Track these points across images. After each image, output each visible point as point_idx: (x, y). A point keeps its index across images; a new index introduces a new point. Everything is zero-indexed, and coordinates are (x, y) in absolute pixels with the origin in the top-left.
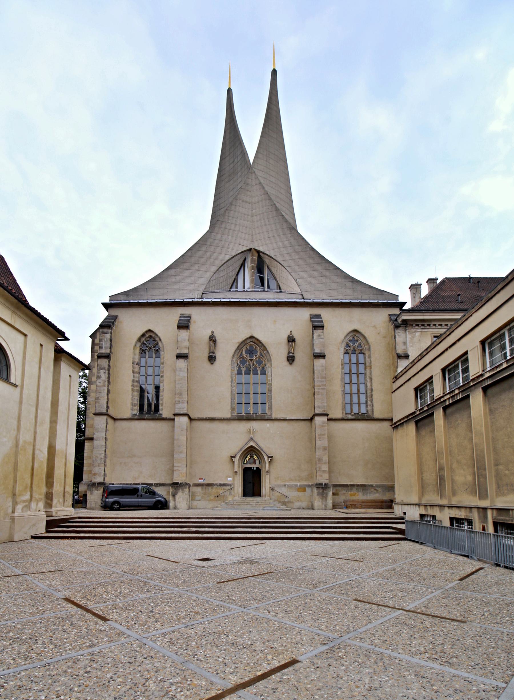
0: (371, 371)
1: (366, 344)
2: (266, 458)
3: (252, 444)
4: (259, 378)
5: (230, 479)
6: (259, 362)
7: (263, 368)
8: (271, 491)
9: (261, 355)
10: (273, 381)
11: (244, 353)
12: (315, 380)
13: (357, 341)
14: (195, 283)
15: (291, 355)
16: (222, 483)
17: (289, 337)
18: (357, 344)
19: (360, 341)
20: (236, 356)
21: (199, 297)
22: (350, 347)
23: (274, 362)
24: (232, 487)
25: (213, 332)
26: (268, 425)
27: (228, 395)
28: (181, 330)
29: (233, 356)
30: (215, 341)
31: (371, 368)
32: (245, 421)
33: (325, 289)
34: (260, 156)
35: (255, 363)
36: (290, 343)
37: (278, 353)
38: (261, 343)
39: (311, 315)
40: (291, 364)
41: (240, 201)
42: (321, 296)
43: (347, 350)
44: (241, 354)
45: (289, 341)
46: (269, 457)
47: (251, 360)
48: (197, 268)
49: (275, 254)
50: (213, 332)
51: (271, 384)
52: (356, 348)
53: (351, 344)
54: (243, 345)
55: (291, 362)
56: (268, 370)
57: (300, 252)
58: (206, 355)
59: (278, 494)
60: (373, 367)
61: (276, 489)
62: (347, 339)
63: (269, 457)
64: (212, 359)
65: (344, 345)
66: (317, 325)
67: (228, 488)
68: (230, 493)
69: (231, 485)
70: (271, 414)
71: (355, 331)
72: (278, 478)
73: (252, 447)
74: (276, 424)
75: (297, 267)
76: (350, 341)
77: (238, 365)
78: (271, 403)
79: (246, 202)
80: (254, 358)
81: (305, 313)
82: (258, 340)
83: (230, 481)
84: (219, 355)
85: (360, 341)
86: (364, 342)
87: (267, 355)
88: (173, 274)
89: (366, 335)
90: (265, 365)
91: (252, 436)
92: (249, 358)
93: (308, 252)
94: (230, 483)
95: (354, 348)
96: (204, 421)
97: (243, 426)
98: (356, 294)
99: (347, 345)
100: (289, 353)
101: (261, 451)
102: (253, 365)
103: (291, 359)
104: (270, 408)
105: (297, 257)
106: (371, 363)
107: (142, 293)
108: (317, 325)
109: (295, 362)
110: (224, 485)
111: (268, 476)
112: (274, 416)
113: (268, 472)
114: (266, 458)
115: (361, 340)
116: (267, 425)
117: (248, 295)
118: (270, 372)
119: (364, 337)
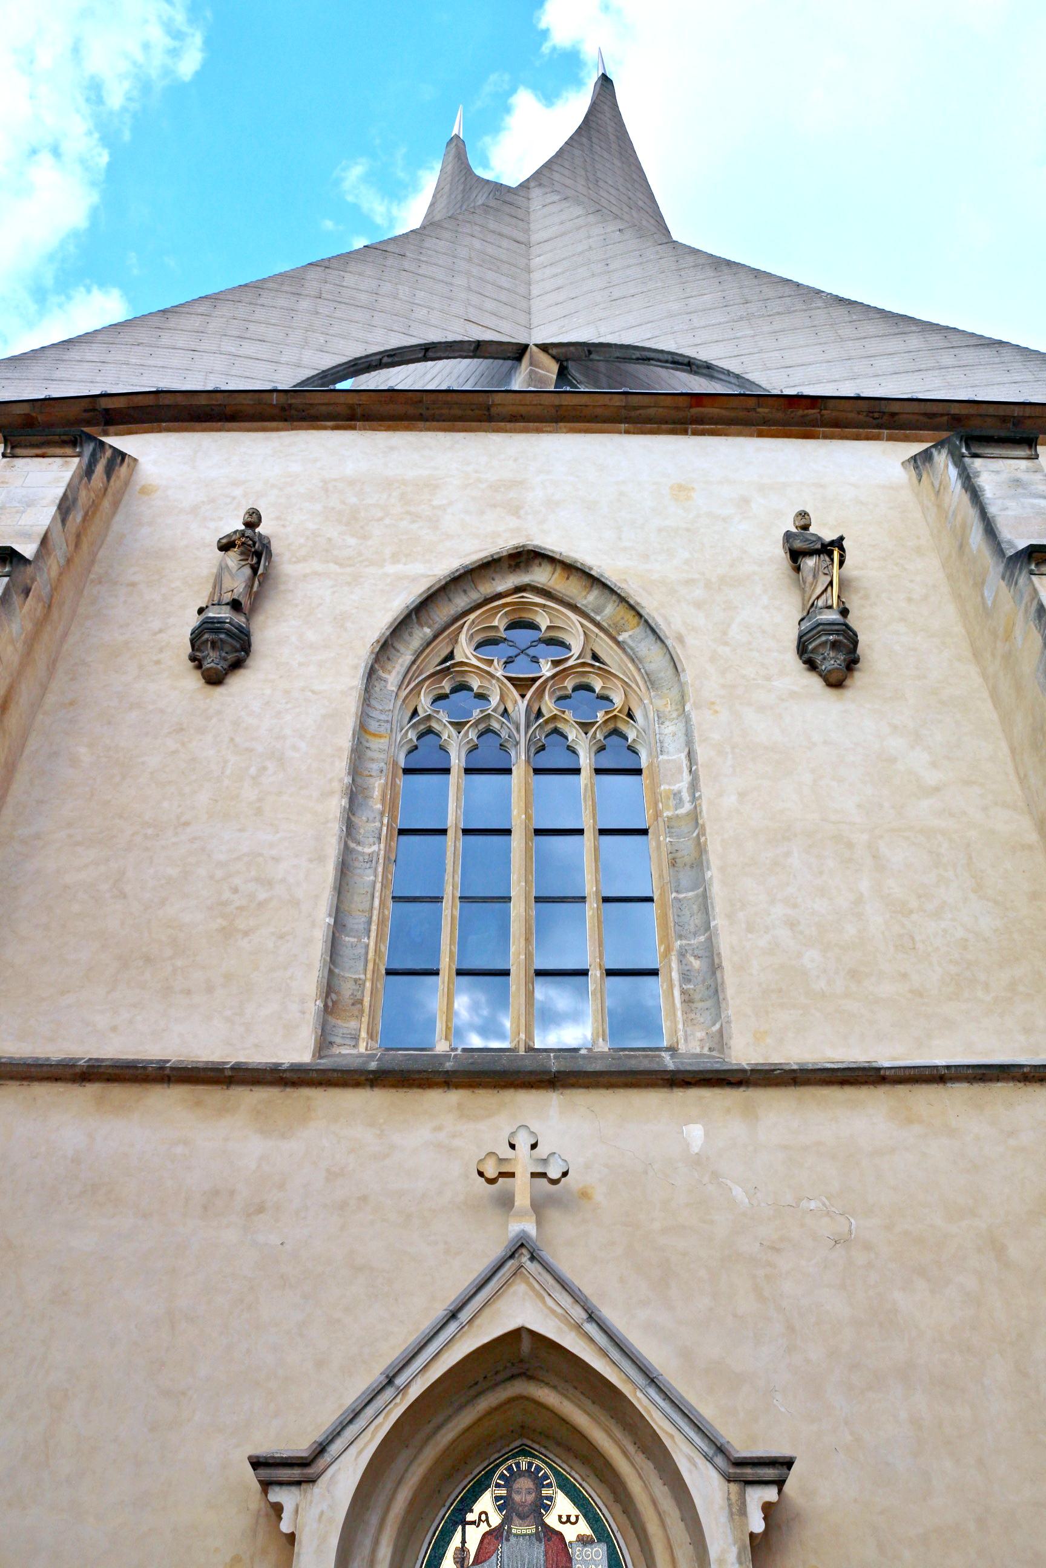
2: (706, 1484)
3: (521, 1310)
4: (583, 799)
6: (581, 686)
26: (695, 1133)
29: (385, 648)
32: (454, 1097)
35: (549, 706)
40: (836, 682)
45: (796, 556)
54: (461, 602)
56: (659, 739)
57: (778, 313)
73: (521, 1356)
74: (777, 1109)
82: (570, 568)
84: (275, 633)
87: (648, 649)
91: (526, 1225)
96: (40, 1090)
97: (438, 1142)
101: (642, 1400)
104: (708, 988)
109: (859, 678)
112: (743, 1054)
114: (706, 1484)
116: (693, 1126)
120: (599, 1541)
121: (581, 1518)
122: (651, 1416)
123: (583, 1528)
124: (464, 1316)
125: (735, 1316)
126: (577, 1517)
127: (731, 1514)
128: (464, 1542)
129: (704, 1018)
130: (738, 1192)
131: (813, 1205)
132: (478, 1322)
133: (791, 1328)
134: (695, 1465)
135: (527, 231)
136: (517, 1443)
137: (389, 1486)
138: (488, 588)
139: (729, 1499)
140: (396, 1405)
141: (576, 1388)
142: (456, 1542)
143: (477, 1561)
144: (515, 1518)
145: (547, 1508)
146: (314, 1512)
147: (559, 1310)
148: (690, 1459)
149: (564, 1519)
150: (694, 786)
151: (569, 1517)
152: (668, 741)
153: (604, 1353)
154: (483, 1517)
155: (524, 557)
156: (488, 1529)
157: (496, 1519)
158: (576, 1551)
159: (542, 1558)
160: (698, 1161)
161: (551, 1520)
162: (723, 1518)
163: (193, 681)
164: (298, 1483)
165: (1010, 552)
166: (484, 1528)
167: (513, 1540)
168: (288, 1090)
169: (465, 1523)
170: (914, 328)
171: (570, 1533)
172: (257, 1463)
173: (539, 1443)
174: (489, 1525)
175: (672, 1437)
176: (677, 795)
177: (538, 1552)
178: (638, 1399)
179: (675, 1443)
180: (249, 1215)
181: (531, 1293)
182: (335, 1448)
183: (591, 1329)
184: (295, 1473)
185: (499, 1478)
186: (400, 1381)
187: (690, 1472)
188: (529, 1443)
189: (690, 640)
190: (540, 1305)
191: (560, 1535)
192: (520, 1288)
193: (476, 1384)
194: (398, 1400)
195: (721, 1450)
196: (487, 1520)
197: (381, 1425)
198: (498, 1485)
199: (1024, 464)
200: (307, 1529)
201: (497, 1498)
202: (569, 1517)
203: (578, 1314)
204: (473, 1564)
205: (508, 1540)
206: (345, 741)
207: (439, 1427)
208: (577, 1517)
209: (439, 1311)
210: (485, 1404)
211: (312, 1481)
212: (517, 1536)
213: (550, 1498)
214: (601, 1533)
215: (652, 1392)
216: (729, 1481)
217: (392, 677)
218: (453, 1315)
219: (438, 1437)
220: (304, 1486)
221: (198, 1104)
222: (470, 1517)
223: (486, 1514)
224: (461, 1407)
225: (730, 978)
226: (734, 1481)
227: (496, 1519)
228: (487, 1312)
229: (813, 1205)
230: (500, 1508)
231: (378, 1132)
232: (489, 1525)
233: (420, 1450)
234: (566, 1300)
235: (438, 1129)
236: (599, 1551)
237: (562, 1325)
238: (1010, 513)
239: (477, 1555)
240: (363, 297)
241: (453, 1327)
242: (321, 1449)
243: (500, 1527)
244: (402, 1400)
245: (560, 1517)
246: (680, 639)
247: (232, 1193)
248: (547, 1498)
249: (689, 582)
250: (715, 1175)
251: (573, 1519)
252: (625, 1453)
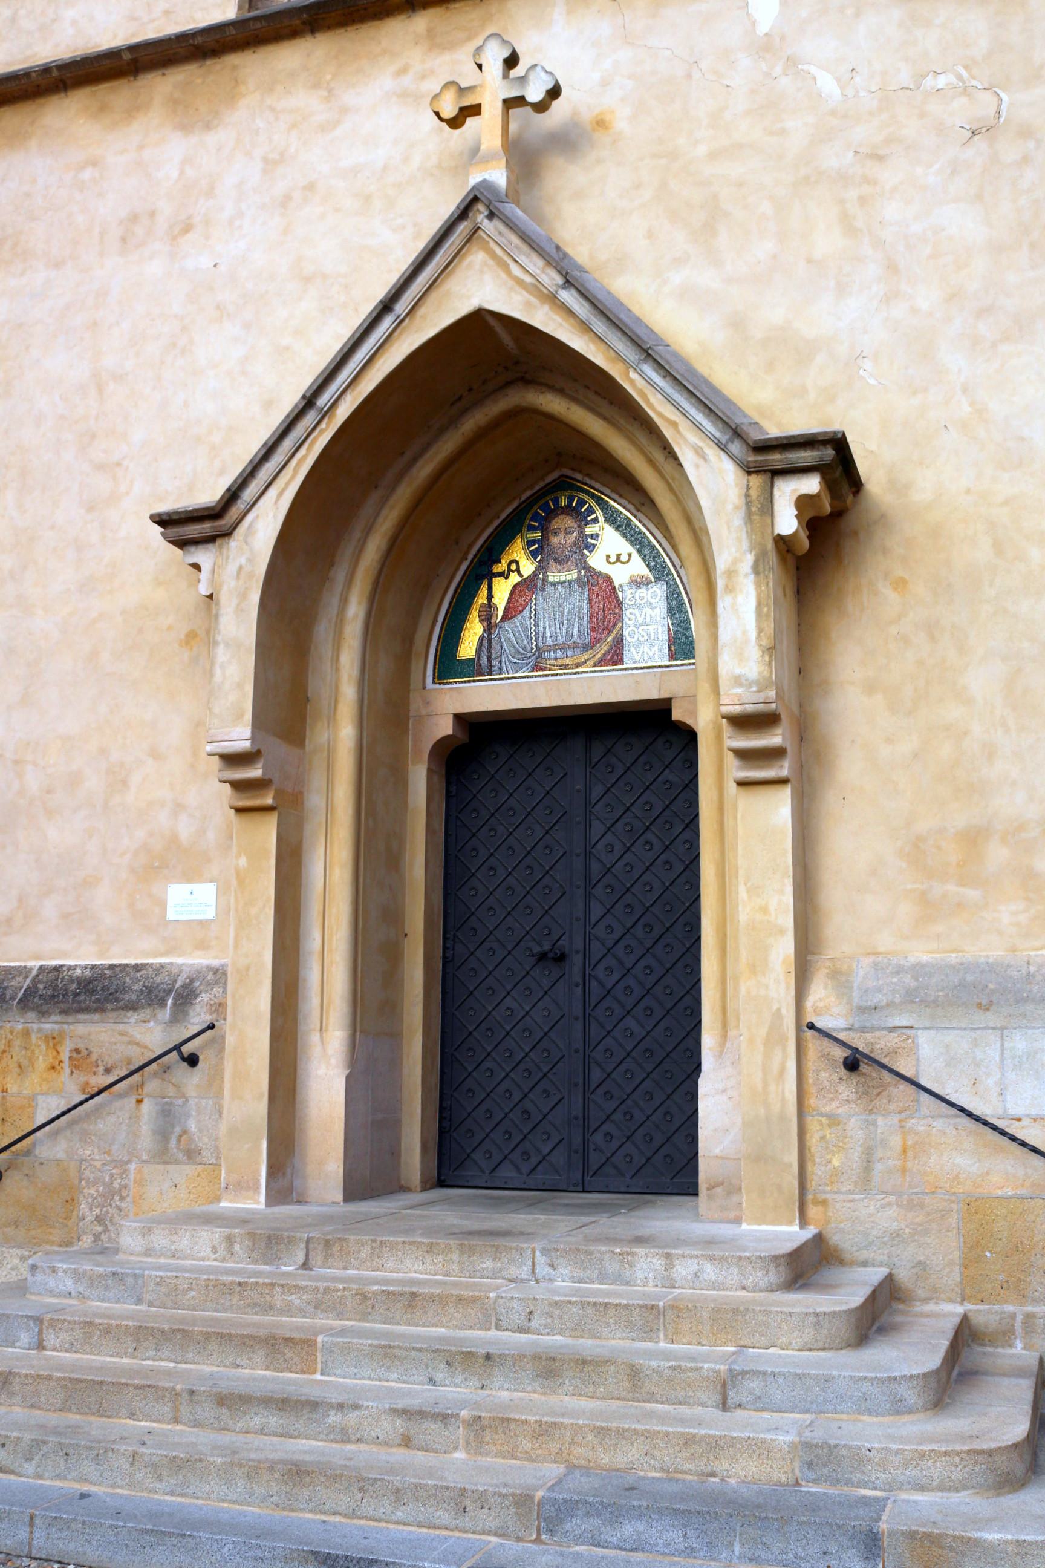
2: (715, 480)
5: (191, 900)
8: (838, 1095)
16: (80, 955)
24: (198, 1018)
46: (768, 458)
59: (962, 1162)
61: (931, 1055)
63: (768, 458)
67: (150, 1033)
68: (168, 1119)
69: (186, 996)
72: (973, 839)
83: (199, 931)
94: (189, 960)
101: (640, 384)
110: (95, 992)
111: (779, 808)
113: (788, 738)
120: (658, 579)
121: (636, 556)
122: (647, 401)
123: (638, 567)
124: (401, 307)
125: (809, 261)
126: (630, 555)
127: (749, 514)
128: (490, 596)
130: (827, 84)
131: (942, 82)
132: (422, 311)
133: (892, 268)
134: (704, 457)
136: (555, 475)
137: (357, 535)
139: (747, 496)
140: (322, 431)
141: (587, 387)
142: (482, 599)
143: (506, 617)
144: (552, 562)
145: (591, 548)
146: (232, 568)
147: (528, 279)
148: (699, 452)
149: (613, 559)
151: (618, 556)
153: (585, 327)
154: (514, 567)
156: (519, 579)
157: (528, 567)
158: (627, 595)
159: (585, 607)
160: (766, 47)
161: (596, 561)
162: (738, 520)
164: (211, 539)
166: (514, 578)
167: (549, 589)
168: (209, 62)
169: (491, 576)
171: (620, 575)
172: (164, 521)
173: (580, 472)
174: (520, 575)
175: (674, 424)
177: (580, 600)
178: (632, 382)
179: (678, 432)
180: (174, 238)
181: (491, 262)
182: (248, 494)
183: (567, 296)
184: (205, 528)
185: (532, 520)
186: (323, 401)
187: (697, 466)
188: (569, 473)
190: (503, 275)
191: (608, 579)
192: (477, 257)
193: (460, 398)
194: (323, 425)
195: (737, 433)
196: (518, 570)
197: (304, 458)
198: (532, 529)
200: (225, 588)
201: (530, 543)
202: (618, 556)
203: (551, 279)
204: (502, 620)
205: (543, 589)
207: (415, 459)
208: (630, 555)
209: (367, 308)
210: (470, 424)
211: (228, 534)
212: (554, 584)
213: (596, 536)
214: (660, 572)
215: (648, 369)
216: (749, 473)
218: (386, 307)
219: (414, 471)
220: (219, 541)
221: (103, 108)
222: (497, 569)
223: (517, 563)
224: (442, 430)
226: (757, 472)
227: (528, 567)
228: (433, 296)
229: (942, 82)
230: (534, 554)
231: (325, 93)
232: (520, 575)
233: (393, 488)
234: (535, 264)
235: (403, 71)
236: (658, 593)
237: (532, 299)
239: (506, 610)
241: (387, 323)
242: (232, 495)
243: (535, 575)
244: (328, 425)
245: (608, 556)
247: (152, 214)
248: (592, 536)
250: (792, 62)
251: (624, 558)
252: (651, 462)
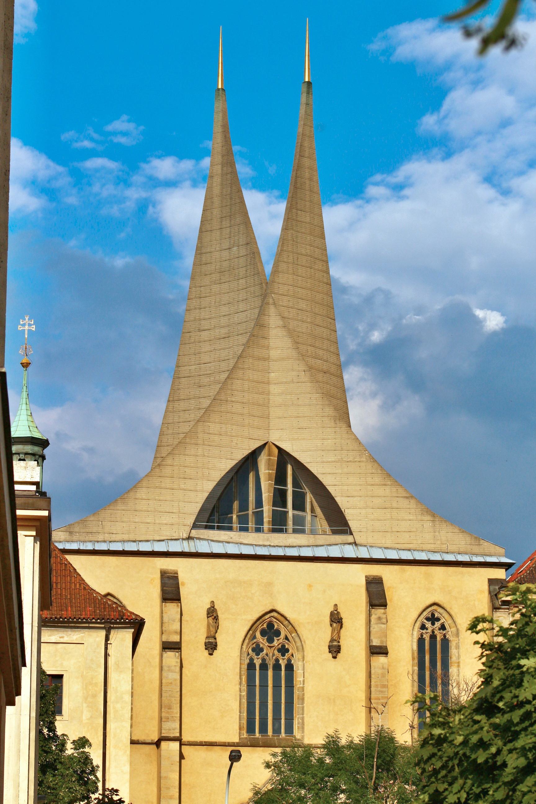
0: (459, 670)
1: (453, 625)
6: (283, 650)
7: (289, 660)
9: (286, 638)
10: (306, 685)
11: (258, 634)
12: (373, 689)
13: (438, 619)
14: (179, 512)
15: (335, 643)
17: (332, 614)
18: (438, 624)
19: (442, 621)
20: (247, 641)
21: (185, 536)
22: (427, 629)
23: (309, 654)
25: (213, 602)
27: (236, 706)
28: (167, 604)
30: (216, 618)
31: (459, 666)
32: (262, 748)
33: (390, 530)
34: (283, 266)
35: (276, 652)
36: (335, 625)
37: (313, 637)
38: (286, 618)
39: (366, 577)
40: (335, 657)
41: (251, 361)
42: (383, 542)
43: (422, 635)
44: (255, 637)
45: (332, 621)
47: (271, 647)
48: (182, 486)
49: (308, 460)
50: (213, 602)
51: (303, 688)
52: (436, 632)
53: (428, 624)
54: (258, 623)
55: (334, 655)
57: (350, 461)
58: (202, 638)
60: (461, 665)
62: (422, 616)
64: (211, 647)
65: (418, 624)
66: (376, 595)
70: (303, 737)
71: (435, 604)
75: (345, 487)
76: (427, 619)
77: (248, 654)
78: (303, 719)
79: (259, 359)
80: (276, 643)
81: (359, 574)
82: (282, 615)
85: (442, 621)
86: (450, 621)
88: (144, 497)
89: (452, 613)
90: (292, 655)
92: (267, 644)
93: (362, 464)
95: (433, 632)
98: (439, 542)
99: (423, 627)
100: (332, 640)
102: (273, 655)
103: (335, 650)
105: (345, 470)
106: (459, 657)
107: (95, 530)
108: (376, 595)
109: (339, 655)
115: (445, 619)
117: (268, 540)
118: (301, 668)
119: (450, 615)
129: (301, 732)
135: (268, 348)
138: (263, 618)
150: (304, 681)
152: (300, 666)
155: (272, 611)
163: (206, 653)
165: (371, 644)
170: (389, 483)
176: (300, 681)
189: (307, 642)
199: (382, 611)
206: (238, 670)
217: (244, 647)
225: (306, 727)
238: (375, 630)
240: (216, 438)
246: (305, 642)
249: (308, 623)
